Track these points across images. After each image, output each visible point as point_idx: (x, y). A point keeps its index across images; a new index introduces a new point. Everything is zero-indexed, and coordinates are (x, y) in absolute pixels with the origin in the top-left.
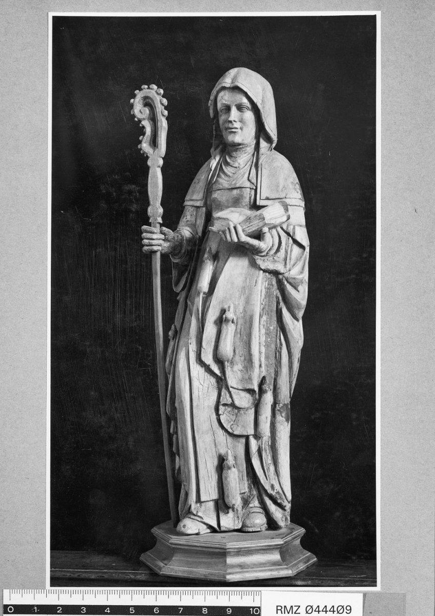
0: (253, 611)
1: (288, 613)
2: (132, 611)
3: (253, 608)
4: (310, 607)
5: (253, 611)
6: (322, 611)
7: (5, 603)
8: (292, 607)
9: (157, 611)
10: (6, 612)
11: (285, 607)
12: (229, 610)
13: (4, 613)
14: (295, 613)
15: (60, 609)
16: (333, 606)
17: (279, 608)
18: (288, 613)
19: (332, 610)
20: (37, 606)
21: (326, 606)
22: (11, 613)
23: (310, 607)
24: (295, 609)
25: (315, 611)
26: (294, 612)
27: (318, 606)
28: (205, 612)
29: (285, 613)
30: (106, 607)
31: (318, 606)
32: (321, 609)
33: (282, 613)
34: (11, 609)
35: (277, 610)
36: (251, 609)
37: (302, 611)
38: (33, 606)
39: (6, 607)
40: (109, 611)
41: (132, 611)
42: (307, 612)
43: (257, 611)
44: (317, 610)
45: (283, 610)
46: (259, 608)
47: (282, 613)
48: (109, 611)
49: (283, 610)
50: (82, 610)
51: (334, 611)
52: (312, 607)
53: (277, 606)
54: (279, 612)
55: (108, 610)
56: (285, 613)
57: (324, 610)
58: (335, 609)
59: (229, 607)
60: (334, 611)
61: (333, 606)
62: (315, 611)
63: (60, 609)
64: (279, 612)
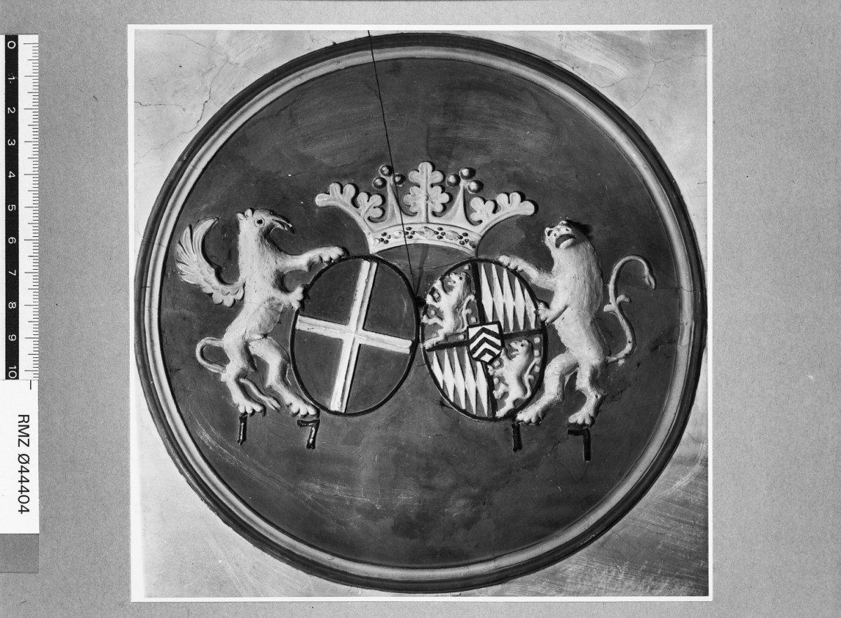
0: (12, 370)
1: (20, 431)
2: (11, 208)
3: (17, 370)
4: (27, 459)
5: (12, 370)
6: (22, 476)
7: (20, 37)
8: (28, 435)
9: (11, 240)
10: (8, 38)
11: (28, 427)
12: (14, 338)
13: (6, 36)
14: (19, 440)
15: (13, 110)
16: (28, 491)
17: (26, 419)
18: (20, 431)
19: (24, 489)
20: (16, 81)
21: (28, 481)
22: (6, 45)
23: (27, 459)
24: (25, 439)
25: (22, 467)
26: (20, 438)
27: (28, 471)
28: (11, 306)
29: (19, 426)
30: (16, 172)
31: (28, 471)
32: (24, 474)
33: (19, 422)
34: (11, 45)
35: (24, 416)
36: (15, 368)
37: (23, 449)
38: (16, 75)
39: (15, 38)
40: (10, 176)
41: (11, 208)
42: (20, 456)
43: (13, 375)
44: (23, 469)
45: (24, 424)
46: (17, 378)
47: (19, 422)
48: (10, 176)
49: (24, 424)
50: (12, 141)
51: (21, 491)
52: (27, 462)
53: (28, 416)
54: (21, 419)
55: (12, 175)
56: (19, 426)
57: (24, 479)
58: (24, 493)
59: (18, 337)
60: (21, 491)
61: (28, 491)
62: (22, 467)
63: (13, 110)
64: (21, 419)
